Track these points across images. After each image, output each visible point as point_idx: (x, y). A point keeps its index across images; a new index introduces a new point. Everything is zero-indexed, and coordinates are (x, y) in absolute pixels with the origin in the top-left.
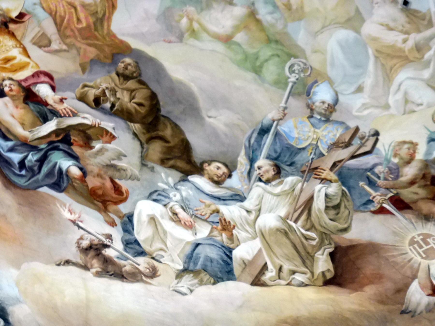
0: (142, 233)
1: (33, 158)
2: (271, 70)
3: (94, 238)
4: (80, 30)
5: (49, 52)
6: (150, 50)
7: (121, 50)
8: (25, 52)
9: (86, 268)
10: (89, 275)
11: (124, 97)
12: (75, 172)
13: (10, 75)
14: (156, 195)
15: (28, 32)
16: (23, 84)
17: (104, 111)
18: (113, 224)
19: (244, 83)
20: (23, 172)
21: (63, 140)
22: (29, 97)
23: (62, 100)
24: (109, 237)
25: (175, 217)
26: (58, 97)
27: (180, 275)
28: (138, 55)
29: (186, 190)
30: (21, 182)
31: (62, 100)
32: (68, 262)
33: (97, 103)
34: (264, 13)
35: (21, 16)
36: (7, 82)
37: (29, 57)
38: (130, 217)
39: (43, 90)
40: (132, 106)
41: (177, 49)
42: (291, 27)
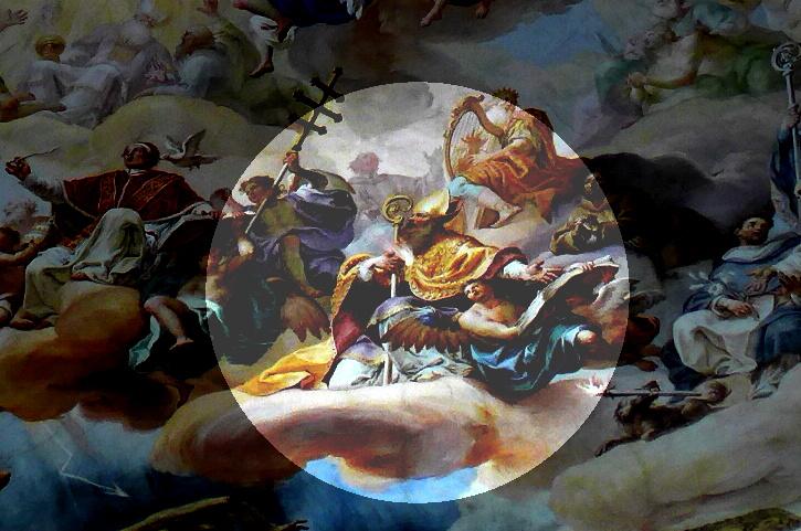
0: (691, 356)
2: (758, 78)
3: (634, 397)
4: (523, 180)
5: (502, 225)
6: (612, 150)
8: (475, 243)
9: (634, 437)
10: (642, 443)
12: (586, 335)
13: (468, 278)
14: (693, 302)
15: (472, 215)
16: (487, 278)
18: (652, 367)
19: (738, 112)
20: (525, 375)
23: (539, 268)
24: (653, 385)
25: (726, 314)
26: (532, 267)
27: (755, 376)
29: (726, 275)
30: (529, 386)
31: (539, 268)
32: (611, 445)
34: (716, 24)
35: (453, 206)
36: (469, 288)
37: (481, 245)
38: (671, 344)
39: (514, 269)
41: (642, 127)
42: (754, 18)
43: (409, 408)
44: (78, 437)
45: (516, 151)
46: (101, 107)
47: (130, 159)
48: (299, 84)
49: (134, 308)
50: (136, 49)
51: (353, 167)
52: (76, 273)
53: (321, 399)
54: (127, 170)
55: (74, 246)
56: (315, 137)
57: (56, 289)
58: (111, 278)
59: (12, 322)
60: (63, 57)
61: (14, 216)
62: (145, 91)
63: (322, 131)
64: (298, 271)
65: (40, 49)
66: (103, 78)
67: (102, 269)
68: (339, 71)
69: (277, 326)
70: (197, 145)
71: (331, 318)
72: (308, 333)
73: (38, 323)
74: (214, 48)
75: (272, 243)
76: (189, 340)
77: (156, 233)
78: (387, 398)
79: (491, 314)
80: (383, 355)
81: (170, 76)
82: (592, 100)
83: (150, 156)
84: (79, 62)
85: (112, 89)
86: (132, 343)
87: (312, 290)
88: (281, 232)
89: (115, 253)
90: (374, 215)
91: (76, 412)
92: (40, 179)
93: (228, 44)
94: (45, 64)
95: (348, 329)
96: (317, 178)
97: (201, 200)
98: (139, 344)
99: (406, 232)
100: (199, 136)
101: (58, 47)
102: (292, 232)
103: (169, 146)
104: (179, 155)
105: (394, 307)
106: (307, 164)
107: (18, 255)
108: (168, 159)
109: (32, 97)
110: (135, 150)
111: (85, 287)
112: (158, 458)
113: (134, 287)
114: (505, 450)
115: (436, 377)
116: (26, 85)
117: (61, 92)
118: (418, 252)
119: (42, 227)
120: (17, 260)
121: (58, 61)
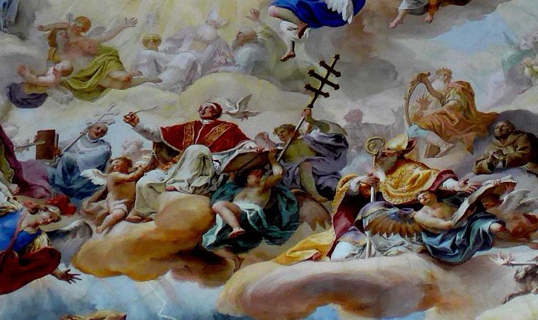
1: (459, 237)
3: (527, 266)
4: (456, 127)
5: (442, 156)
7: (494, 118)
11: (509, 151)
12: (496, 226)
13: (420, 190)
15: (422, 150)
16: (432, 189)
17: (500, 170)
20: (457, 251)
21: (479, 209)
22: (440, 195)
23: (465, 183)
26: (461, 182)
28: (506, 116)
30: (458, 259)
31: (465, 183)
32: (511, 296)
33: (492, 168)
35: (410, 144)
36: (420, 196)
37: (429, 168)
39: (450, 184)
40: (518, 154)
43: (382, 273)
44: (170, 292)
45: (451, 108)
46: (184, 80)
47: (203, 114)
48: (312, 65)
49: (206, 209)
50: (207, 43)
51: (347, 118)
52: (168, 186)
53: (325, 267)
54: (201, 120)
55: (167, 169)
56: (321, 98)
57: (156, 197)
58: (191, 190)
59: (128, 217)
60: (160, 48)
61: (128, 150)
62: (214, 70)
63: (327, 95)
64: (311, 186)
65: (146, 43)
66: (186, 61)
67: (186, 184)
68: (337, 57)
69: (296, 220)
70: (246, 104)
71: (332, 215)
72: (317, 224)
73: (143, 219)
74: (256, 42)
75: (293, 166)
76: (241, 230)
77: (221, 160)
78: (369, 266)
79: (435, 212)
80: (366, 238)
81: (229, 60)
82: (500, 76)
83: (217, 111)
84: (170, 51)
85: (192, 69)
86: (205, 231)
87: (320, 198)
88: (299, 160)
89: (194, 174)
90: (360, 149)
91: (168, 276)
92: (146, 127)
93: (266, 39)
94: (149, 52)
95: (344, 222)
96: (323, 126)
97: (249, 139)
98: (209, 232)
99: (380, 158)
100: (248, 98)
101: (157, 41)
102: (308, 160)
103: (228, 105)
104: (235, 111)
105: (372, 210)
106: (316, 116)
107: (131, 175)
108: (228, 113)
109: (141, 73)
110: (206, 108)
111: (174, 195)
112: (222, 304)
113: (206, 195)
114: (444, 300)
115: (399, 253)
116: (136, 66)
117: (159, 70)
118: (389, 172)
119: (147, 157)
120: (131, 178)
121: (157, 50)
